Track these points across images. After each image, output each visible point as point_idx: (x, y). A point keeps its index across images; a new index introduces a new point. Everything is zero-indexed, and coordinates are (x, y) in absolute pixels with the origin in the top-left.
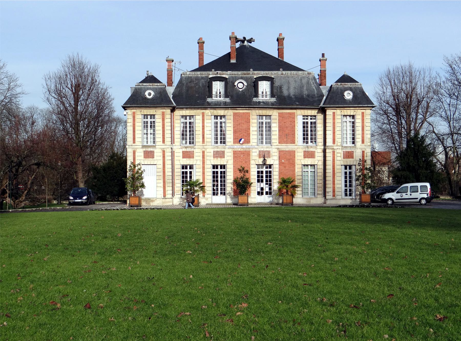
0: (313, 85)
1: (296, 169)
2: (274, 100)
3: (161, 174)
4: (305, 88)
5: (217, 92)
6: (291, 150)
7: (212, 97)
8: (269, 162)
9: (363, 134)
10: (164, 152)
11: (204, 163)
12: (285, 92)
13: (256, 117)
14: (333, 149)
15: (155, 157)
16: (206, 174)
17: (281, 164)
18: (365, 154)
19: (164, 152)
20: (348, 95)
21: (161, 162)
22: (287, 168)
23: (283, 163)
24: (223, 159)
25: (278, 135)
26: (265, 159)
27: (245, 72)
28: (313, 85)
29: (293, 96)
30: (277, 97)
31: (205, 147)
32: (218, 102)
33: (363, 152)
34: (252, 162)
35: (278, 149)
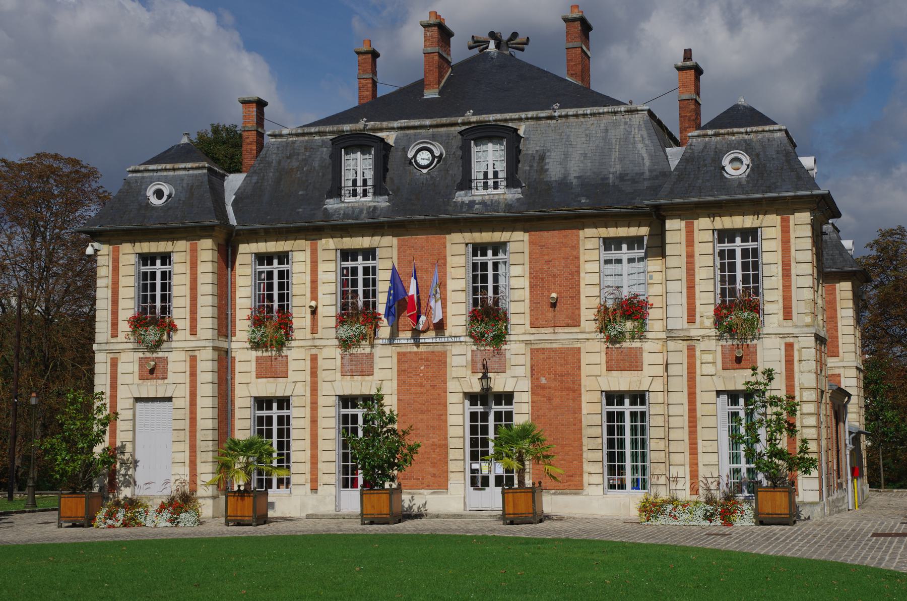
0: (640, 145)
1: (584, 405)
2: (514, 195)
3: (186, 424)
4: (615, 155)
5: (355, 182)
6: (566, 345)
7: (340, 196)
8: (499, 384)
9: (787, 287)
10: (193, 359)
11: (314, 390)
12: (554, 171)
13: (461, 249)
14: (689, 338)
15: (170, 374)
16: (321, 423)
17: (536, 389)
18: (796, 354)
19: (193, 359)
20: (736, 168)
21: (185, 391)
22: (555, 403)
23: (543, 388)
24: (367, 378)
25: (527, 301)
26: (485, 377)
27: (444, 120)
28: (640, 145)
29: (575, 182)
30: (529, 186)
31: (318, 343)
32: (353, 208)
33: (789, 347)
34: (452, 386)
35: (528, 342)
